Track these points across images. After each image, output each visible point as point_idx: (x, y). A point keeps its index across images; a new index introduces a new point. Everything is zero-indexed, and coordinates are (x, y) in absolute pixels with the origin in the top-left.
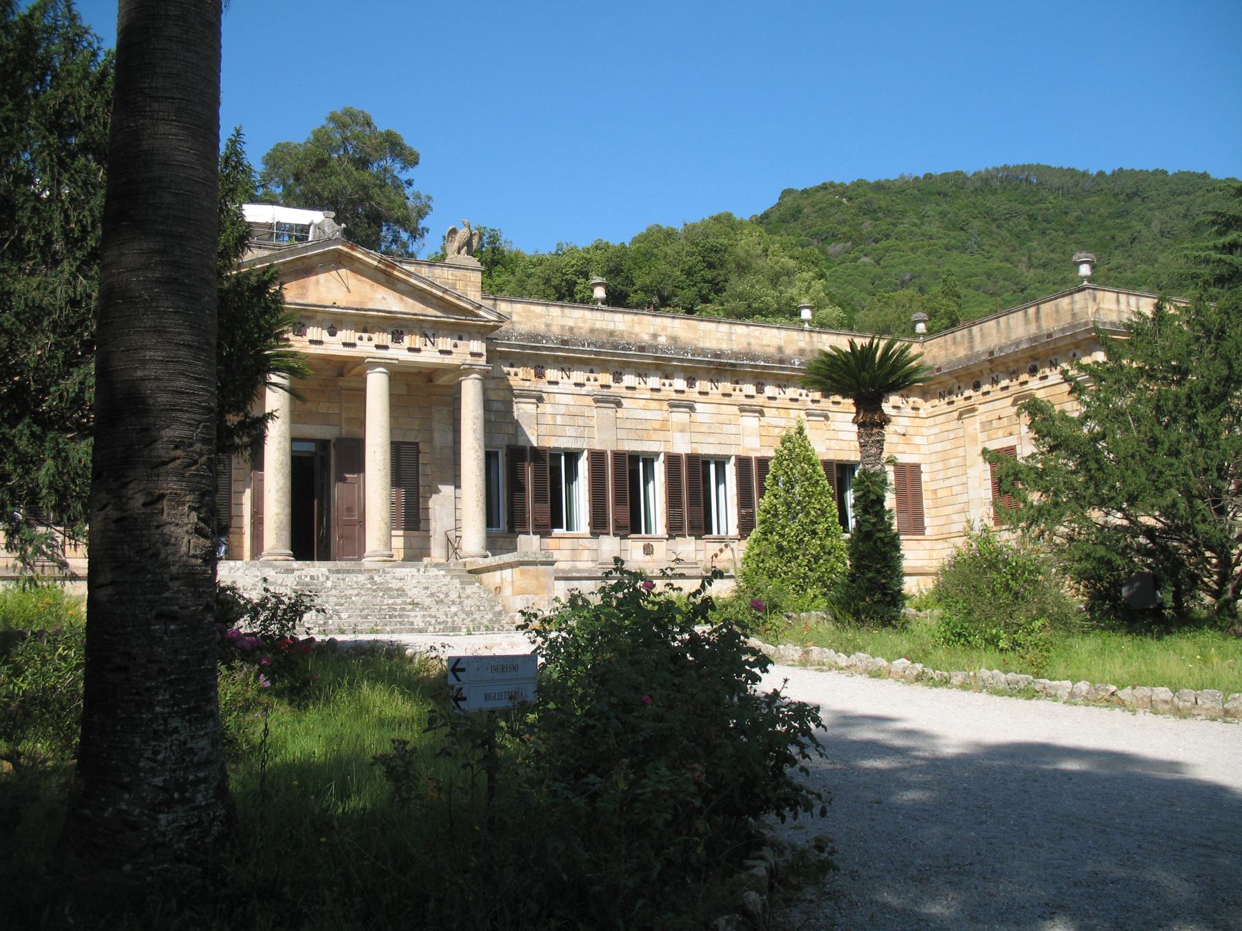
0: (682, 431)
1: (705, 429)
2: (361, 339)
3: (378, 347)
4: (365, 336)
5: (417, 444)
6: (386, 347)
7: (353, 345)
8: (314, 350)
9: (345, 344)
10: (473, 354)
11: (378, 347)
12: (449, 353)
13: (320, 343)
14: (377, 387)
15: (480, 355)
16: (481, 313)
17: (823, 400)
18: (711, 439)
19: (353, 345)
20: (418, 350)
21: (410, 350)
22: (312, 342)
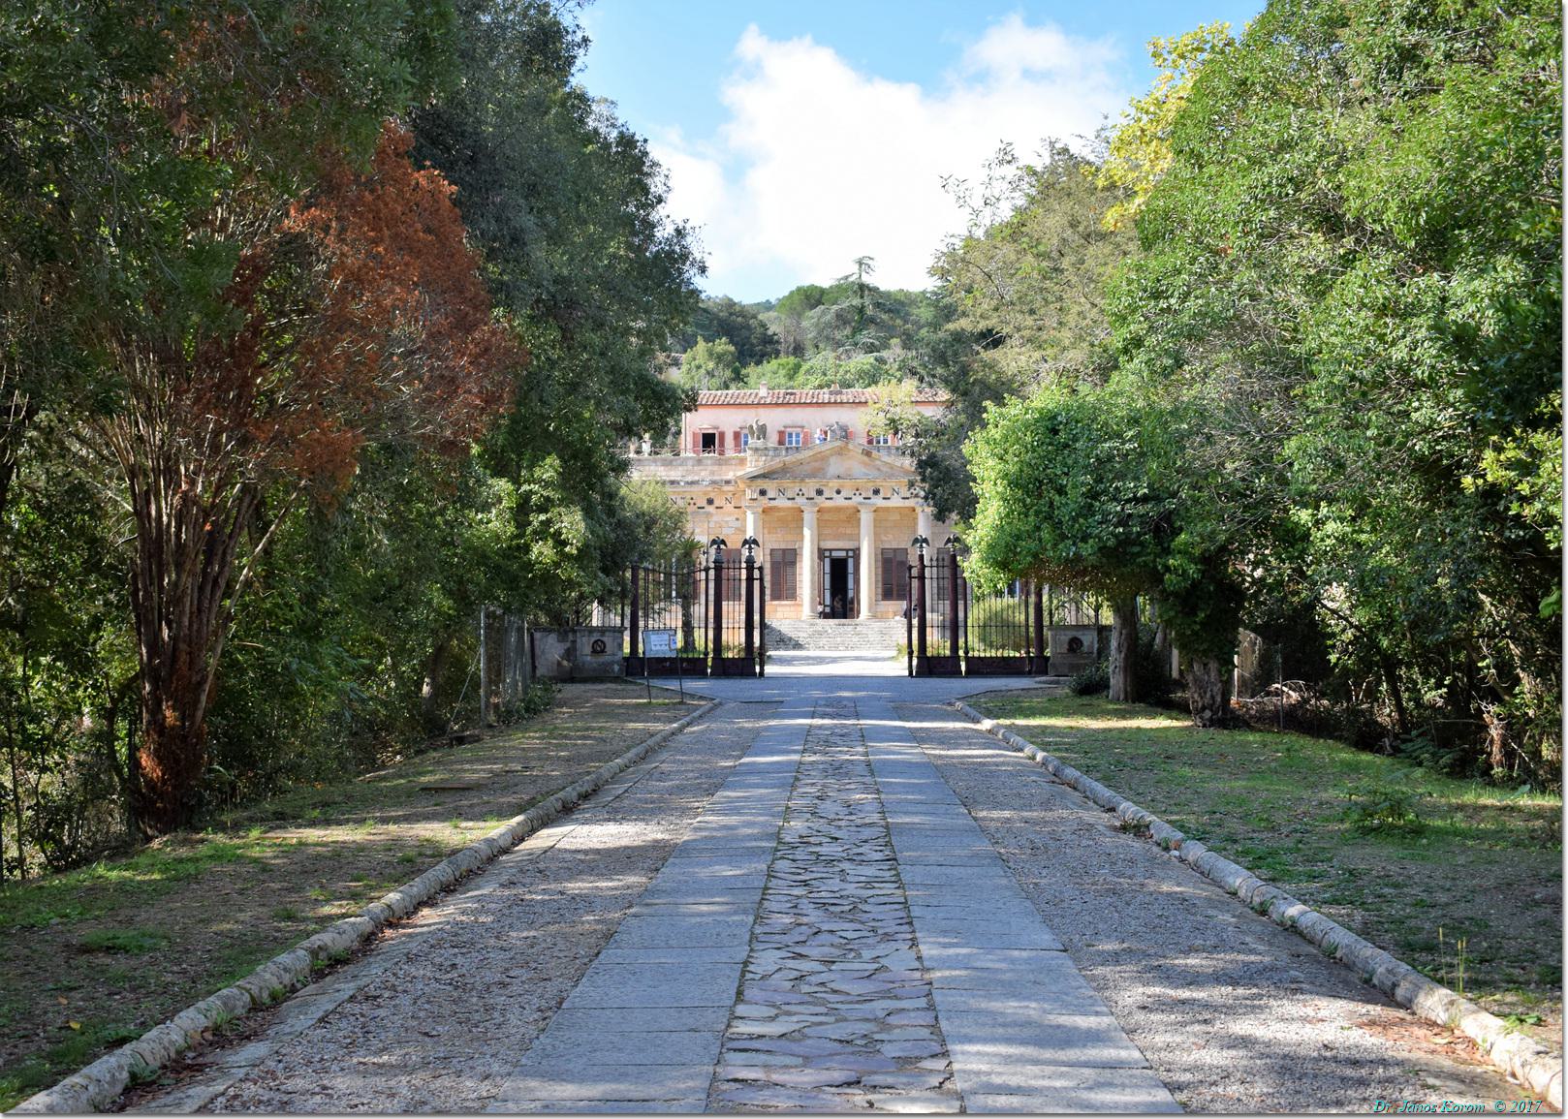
8: (829, 504)
14: (866, 518)
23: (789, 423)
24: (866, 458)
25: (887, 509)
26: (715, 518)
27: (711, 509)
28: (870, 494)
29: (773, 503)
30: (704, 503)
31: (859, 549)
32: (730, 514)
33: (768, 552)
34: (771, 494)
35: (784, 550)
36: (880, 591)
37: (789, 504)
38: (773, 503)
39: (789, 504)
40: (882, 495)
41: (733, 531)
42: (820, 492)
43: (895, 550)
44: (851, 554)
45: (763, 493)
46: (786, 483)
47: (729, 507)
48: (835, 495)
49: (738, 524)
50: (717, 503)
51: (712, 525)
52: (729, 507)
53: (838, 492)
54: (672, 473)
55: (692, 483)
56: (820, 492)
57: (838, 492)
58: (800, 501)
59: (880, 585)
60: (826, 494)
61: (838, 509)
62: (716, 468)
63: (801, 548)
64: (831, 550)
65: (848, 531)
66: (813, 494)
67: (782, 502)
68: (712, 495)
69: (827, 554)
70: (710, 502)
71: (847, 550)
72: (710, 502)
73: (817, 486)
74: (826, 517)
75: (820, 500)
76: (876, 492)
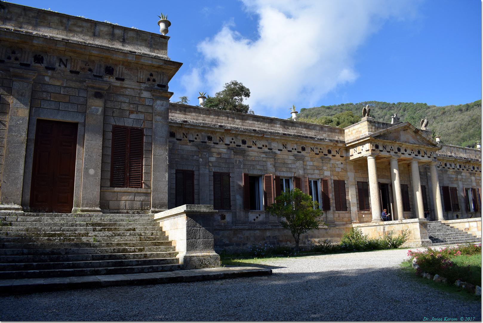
5: (407, 185)
8: (402, 157)
16: (437, 145)
26: (332, 162)
27: (330, 156)
30: (326, 152)
32: (339, 160)
34: (381, 148)
39: (388, 154)
45: (377, 147)
46: (387, 142)
47: (338, 156)
48: (405, 152)
52: (338, 156)
54: (310, 133)
55: (321, 139)
56: (399, 150)
62: (330, 133)
70: (329, 152)
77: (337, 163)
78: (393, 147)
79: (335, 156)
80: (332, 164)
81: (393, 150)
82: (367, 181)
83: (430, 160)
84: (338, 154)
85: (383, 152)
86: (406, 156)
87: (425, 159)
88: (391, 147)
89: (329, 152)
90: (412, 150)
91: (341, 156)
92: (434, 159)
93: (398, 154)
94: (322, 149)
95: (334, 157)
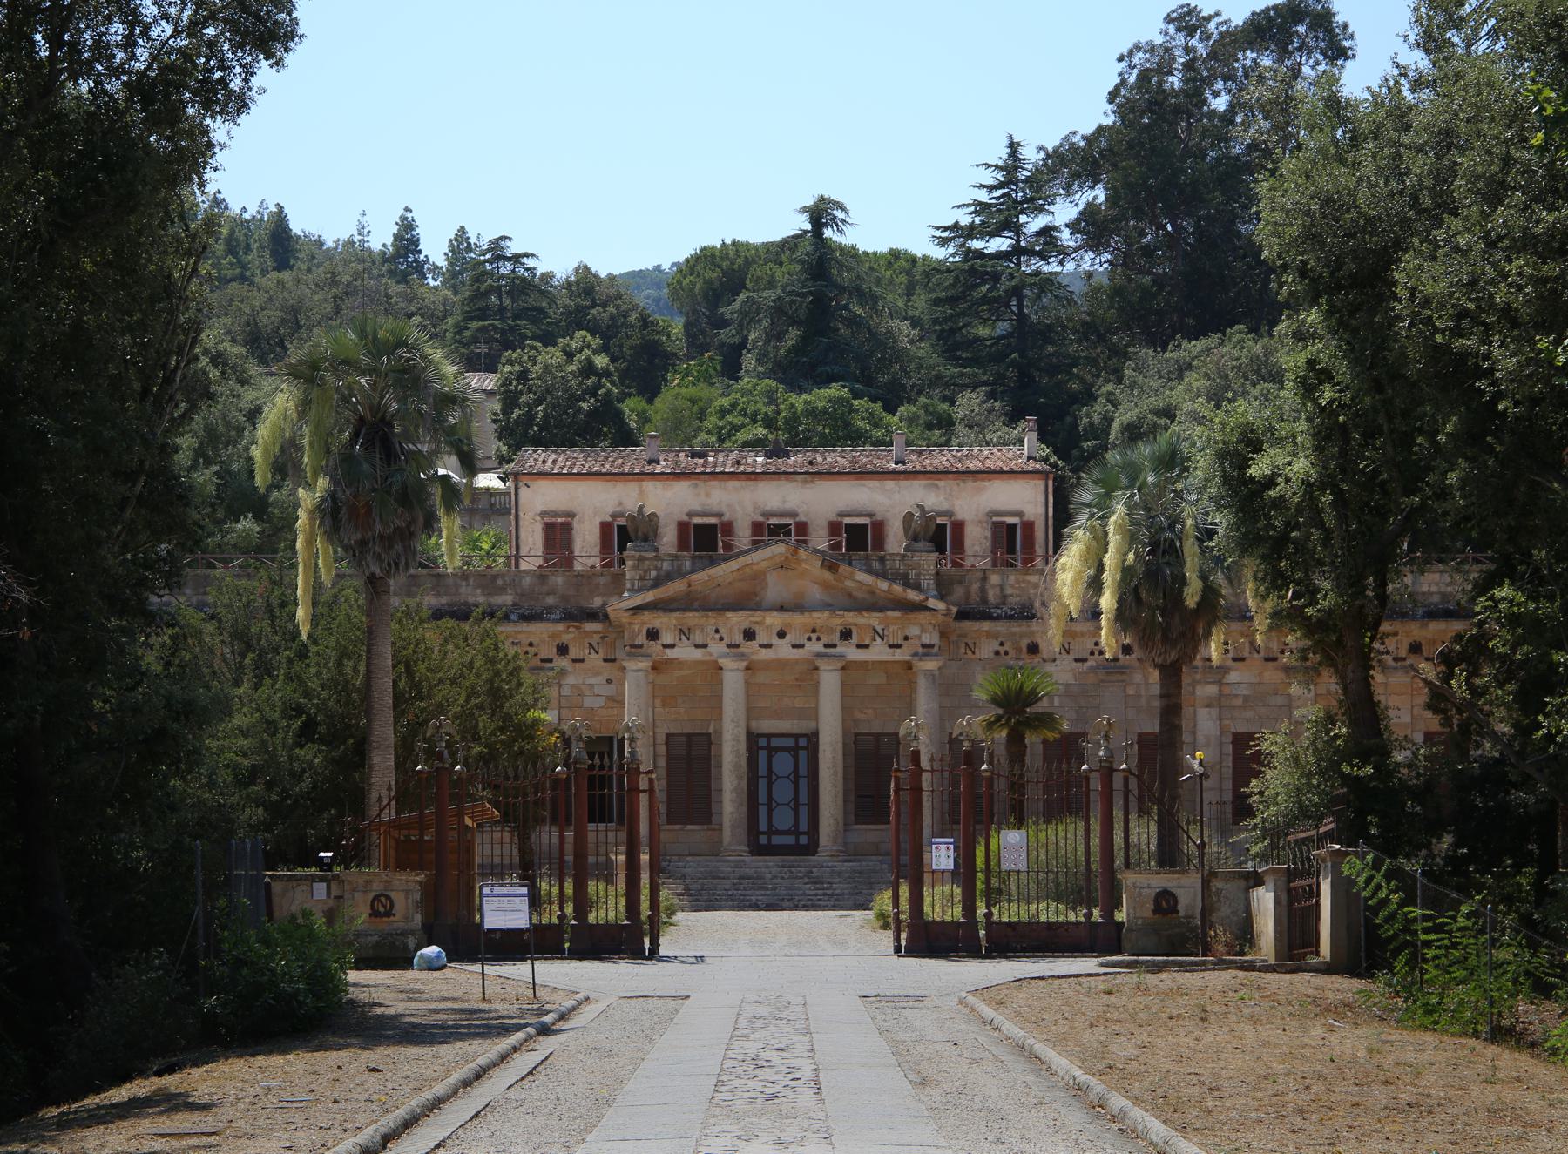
0: (1208, 706)
1: (1239, 702)
2: (809, 639)
3: (826, 646)
4: (814, 636)
6: (834, 646)
7: (802, 646)
8: (765, 654)
9: (794, 646)
10: (923, 646)
11: (826, 646)
12: (899, 646)
13: (769, 646)
14: (830, 681)
15: (932, 646)
17: (1412, 656)
18: (1249, 714)
19: (802, 646)
20: (867, 646)
21: (859, 646)
22: (761, 646)
23: (697, 507)
24: (827, 575)
25: (863, 665)
26: (570, 680)
27: (563, 663)
28: (836, 638)
29: (670, 653)
31: (816, 734)
32: (597, 674)
33: (661, 738)
34: (667, 638)
35: (689, 736)
36: (852, 807)
37: (698, 654)
38: (670, 653)
39: (698, 654)
40: (855, 640)
41: (600, 702)
42: (749, 635)
43: (878, 736)
44: (803, 742)
46: (692, 618)
48: (775, 641)
49: (610, 690)
50: (574, 652)
51: (566, 691)
53: (781, 635)
56: (749, 635)
57: (781, 635)
58: (716, 649)
59: (852, 798)
60: (762, 637)
61: (782, 664)
63: (719, 733)
64: (769, 736)
65: (799, 703)
66: (738, 638)
67: (685, 652)
68: (566, 638)
69: (763, 742)
71: (797, 736)
72: (563, 650)
73: (746, 624)
74: (761, 678)
75: (749, 648)
76: (846, 635)
77: (590, 681)
78: (722, 630)
79: (582, 661)
80: (573, 686)
81: (721, 639)
82: (711, 731)
83: (898, 655)
84: (594, 655)
85: (676, 649)
86: (784, 650)
87: (878, 652)
88: (717, 631)
89: (563, 650)
90: (814, 631)
91: (605, 660)
92: (920, 650)
93: (741, 650)
94: (535, 643)
95: (577, 664)
